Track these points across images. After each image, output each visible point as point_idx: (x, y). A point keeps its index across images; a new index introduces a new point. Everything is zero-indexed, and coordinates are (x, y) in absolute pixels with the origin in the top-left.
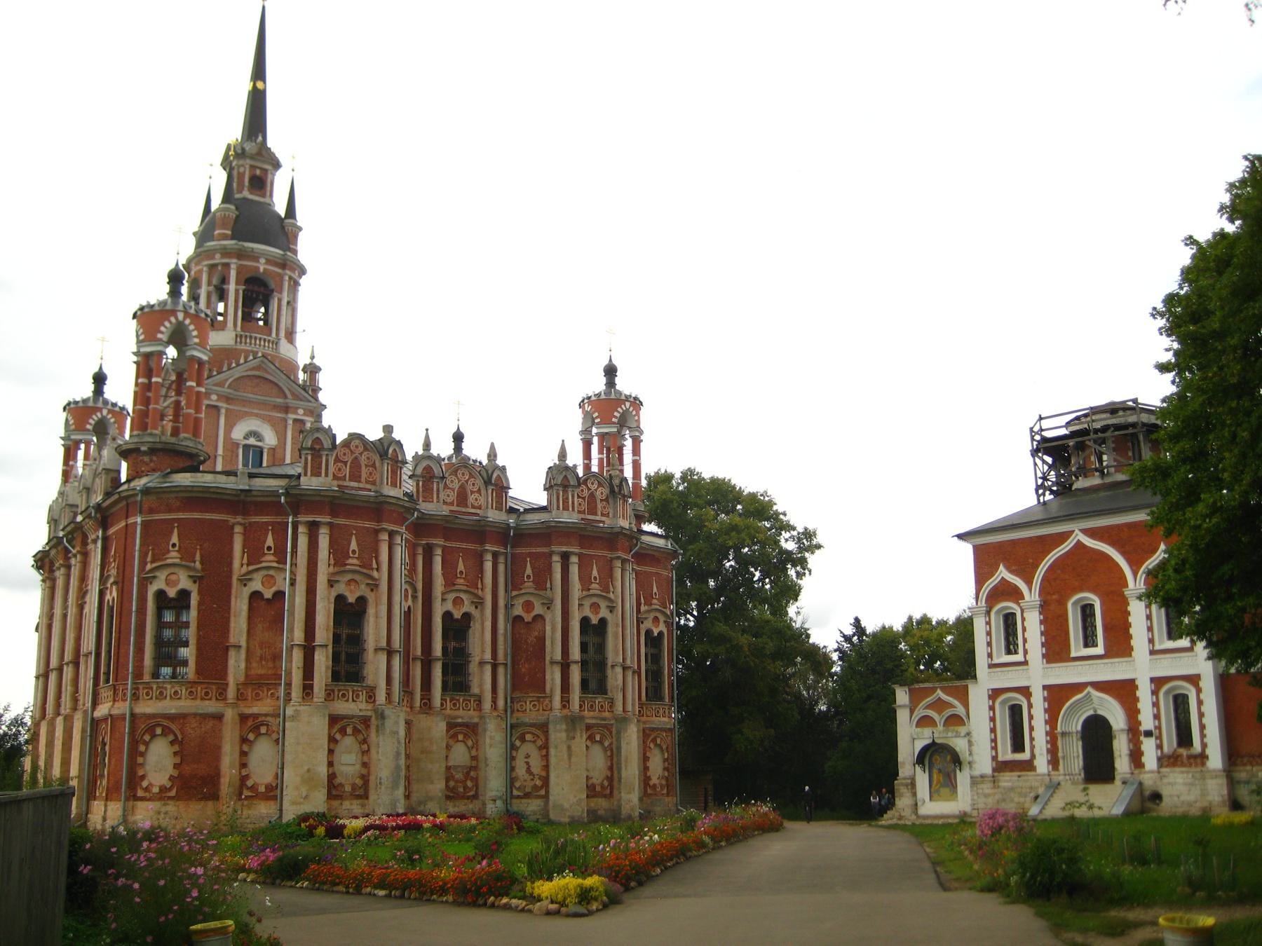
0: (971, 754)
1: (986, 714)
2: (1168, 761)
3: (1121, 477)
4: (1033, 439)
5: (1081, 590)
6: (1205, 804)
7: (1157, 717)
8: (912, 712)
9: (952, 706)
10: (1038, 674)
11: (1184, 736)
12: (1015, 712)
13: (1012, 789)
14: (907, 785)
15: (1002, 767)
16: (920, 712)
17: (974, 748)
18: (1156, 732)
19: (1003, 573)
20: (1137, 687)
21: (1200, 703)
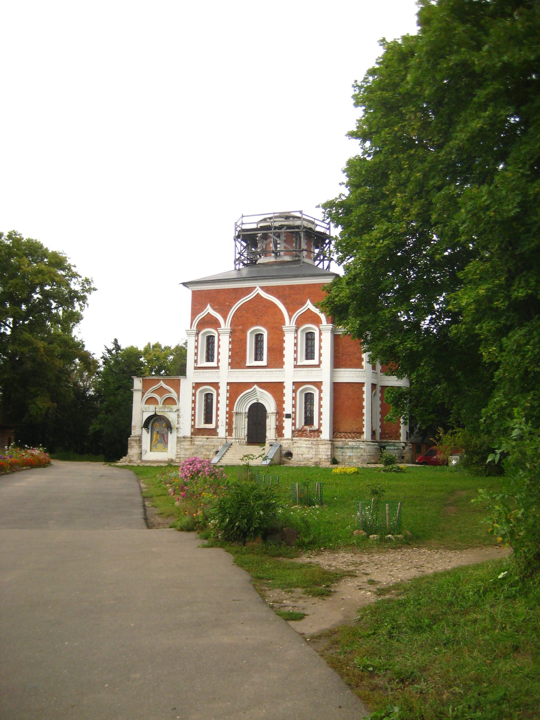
0: (178, 423)
1: (190, 398)
2: (298, 433)
3: (287, 258)
4: (236, 230)
5: (257, 325)
6: (317, 460)
7: (294, 406)
9: (170, 392)
10: (225, 375)
11: (309, 420)
12: (208, 397)
13: (203, 446)
14: (136, 441)
15: (197, 432)
16: (148, 395)
17: (181, 419)
19: (209, 310)
21: (320, 399)
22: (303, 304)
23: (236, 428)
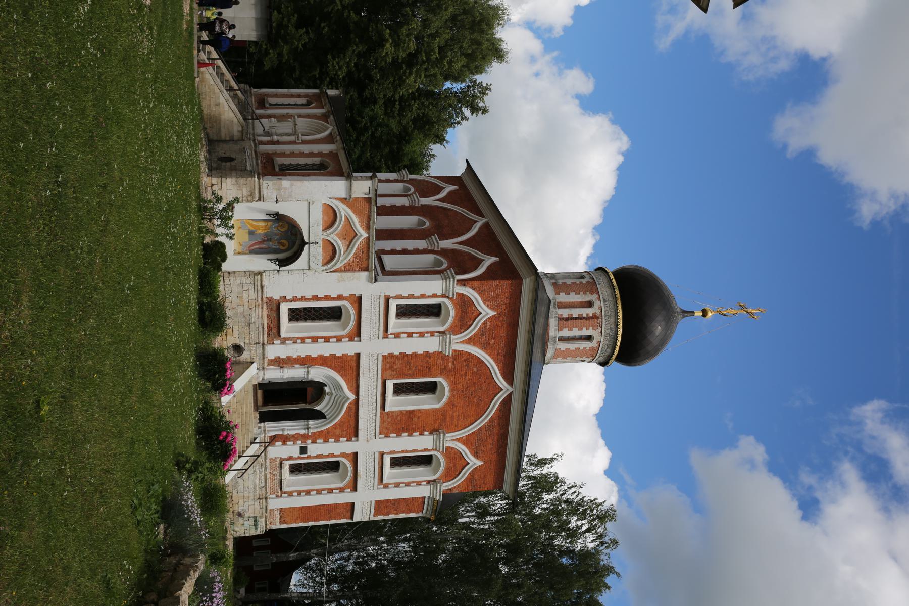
5: (452, 390)
7: (318, 456)
8: (344, 200)
10: (372, 349)
12: (334, 314)
15: (274, 307)
18: (305, 455)
19: (487, 312)
20: (349, 440)
21: (331, 491)
22: (476, 455)
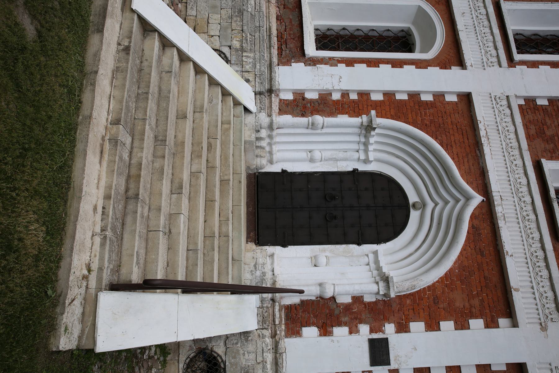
23: (313, 126)
